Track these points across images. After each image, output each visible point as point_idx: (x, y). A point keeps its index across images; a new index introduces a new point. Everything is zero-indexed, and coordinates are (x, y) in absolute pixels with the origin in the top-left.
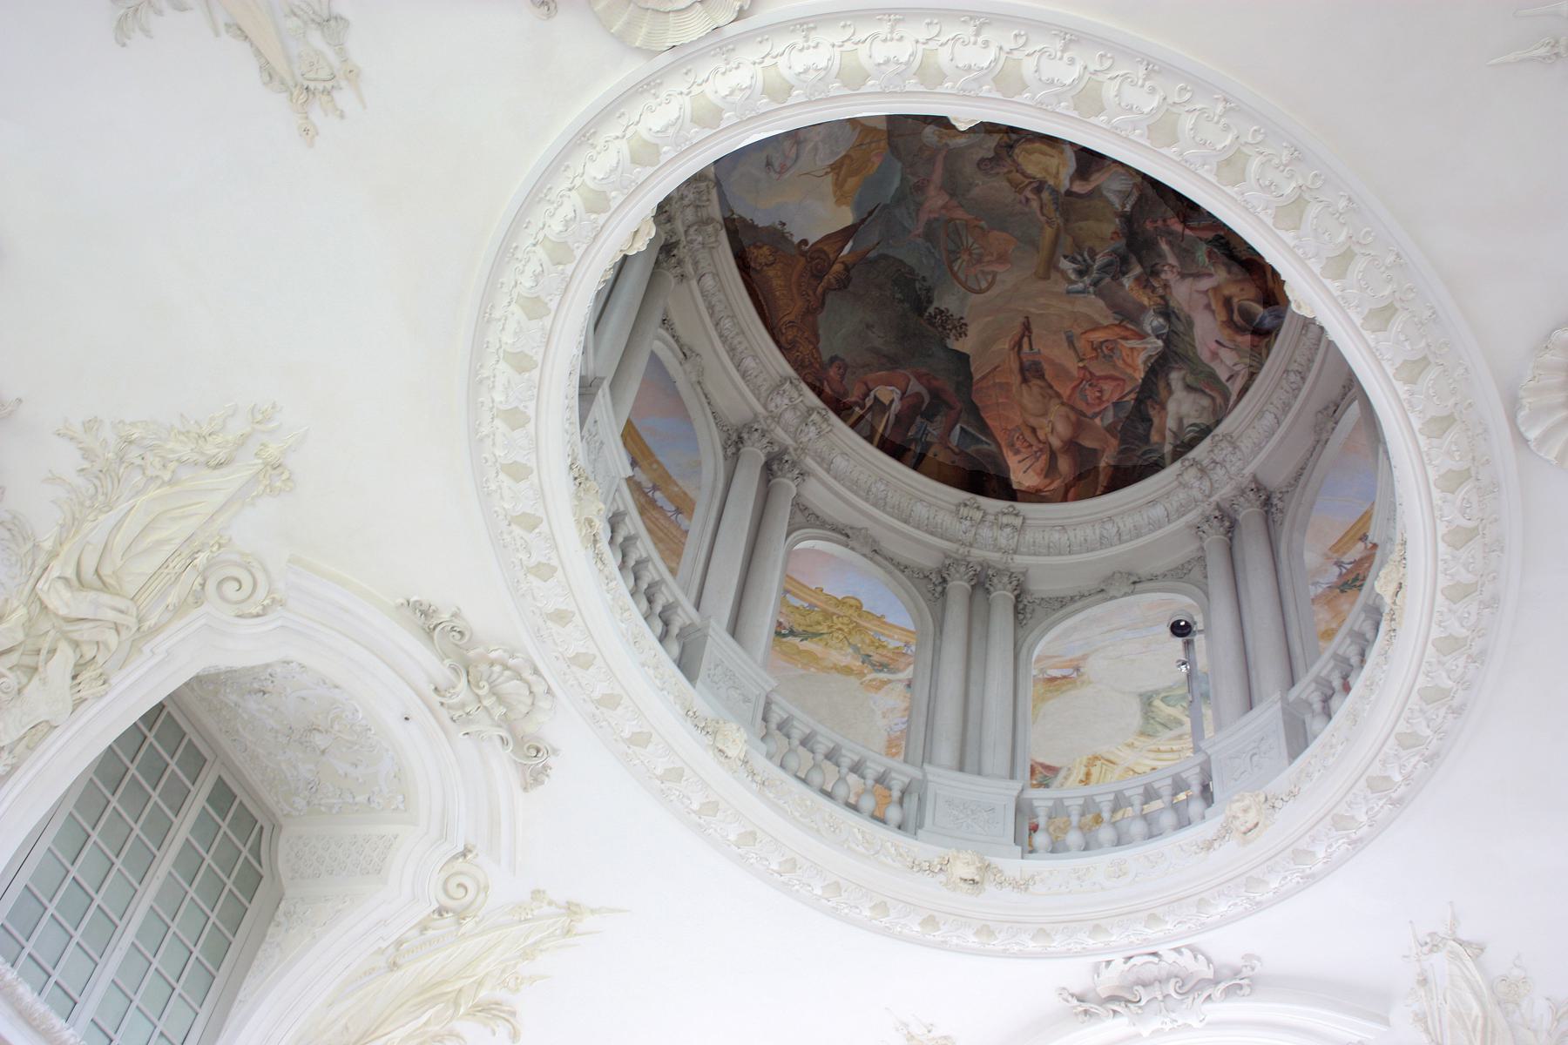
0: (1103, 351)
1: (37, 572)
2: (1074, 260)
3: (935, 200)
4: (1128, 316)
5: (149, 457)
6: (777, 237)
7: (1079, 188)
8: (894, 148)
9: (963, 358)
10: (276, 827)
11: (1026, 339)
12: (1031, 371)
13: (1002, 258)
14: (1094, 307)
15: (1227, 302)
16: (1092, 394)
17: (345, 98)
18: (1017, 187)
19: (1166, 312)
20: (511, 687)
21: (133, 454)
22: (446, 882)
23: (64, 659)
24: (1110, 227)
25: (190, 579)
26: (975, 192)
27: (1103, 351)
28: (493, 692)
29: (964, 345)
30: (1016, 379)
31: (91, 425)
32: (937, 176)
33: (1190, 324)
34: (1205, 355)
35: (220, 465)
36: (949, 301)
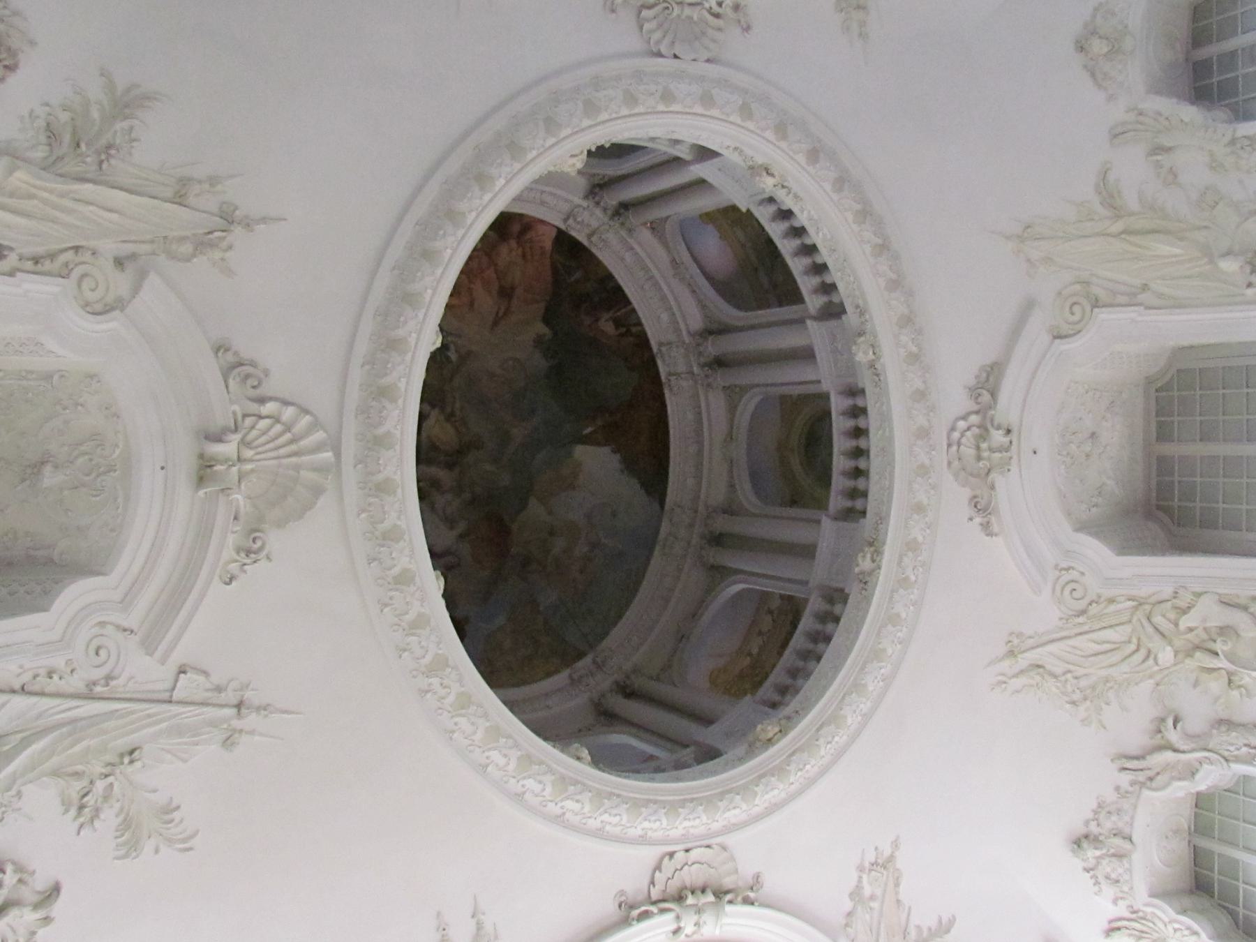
1: (1166, 672)
2: (448, 358)
3: (518, 433)
5: (1069, 689)
6: (630, 465)
9: (546, 320)
10: (1149, 381)
11: (501, 314)
12: (506, 293)
17: (871, 857)
20: (968, 451)
21: (1077, 696)
22: (1080, 321)
23: (1185, 623)
25: (1094, 609)
28: (979, 458)
29: (542, 329)
30: (519, 291)
31: (1085, 722)
35: (1039, 666)
36: (539, 363)
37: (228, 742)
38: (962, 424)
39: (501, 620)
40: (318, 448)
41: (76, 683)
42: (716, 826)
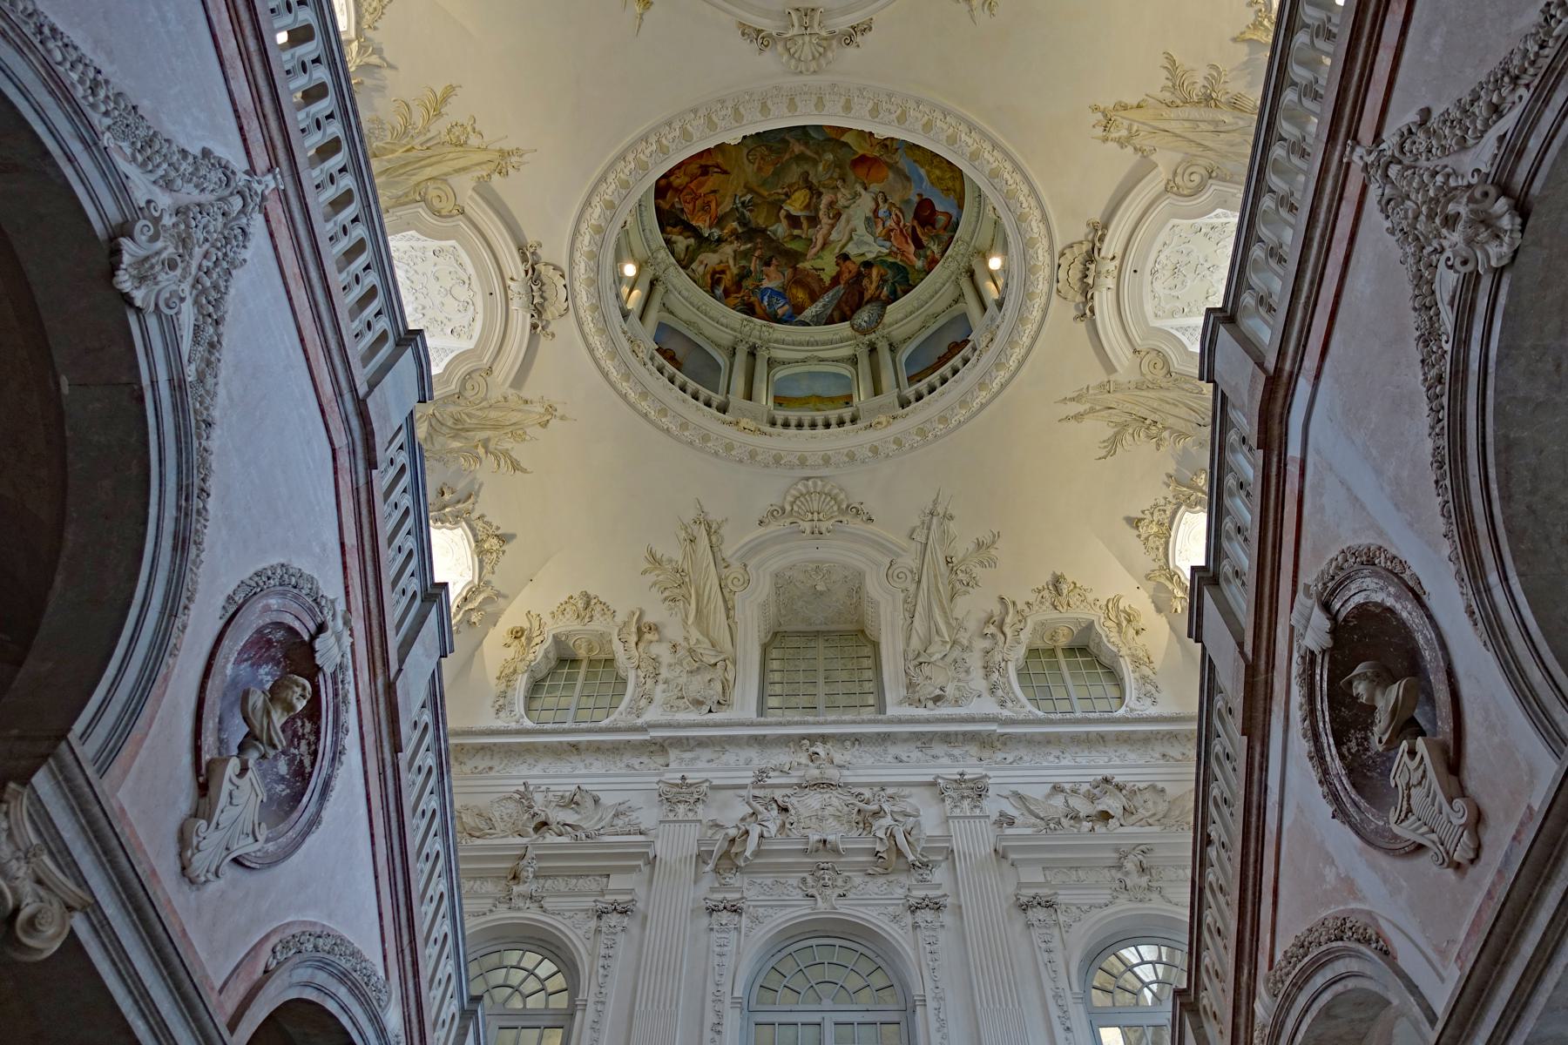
0: (706, 208)
4: (720, 221)
7: (783, 213)
8: (830, 140)
13: (760, 169)
14: (726, 206)
15: (723, 272)
16: (689, 198)
17: (1099, 131)
18: (790, 186)
19: (720, 241)
24: (761, 222)
26: (794, 166)
27: (706, 208)
32: (808, 153)
33: (715, 252)
34: (701, 257)
37: (951, 518)
38: (785, 57)
39: (922, 171)
40: (806, 486)
41: (912, 588)
42: (1048, 260)
